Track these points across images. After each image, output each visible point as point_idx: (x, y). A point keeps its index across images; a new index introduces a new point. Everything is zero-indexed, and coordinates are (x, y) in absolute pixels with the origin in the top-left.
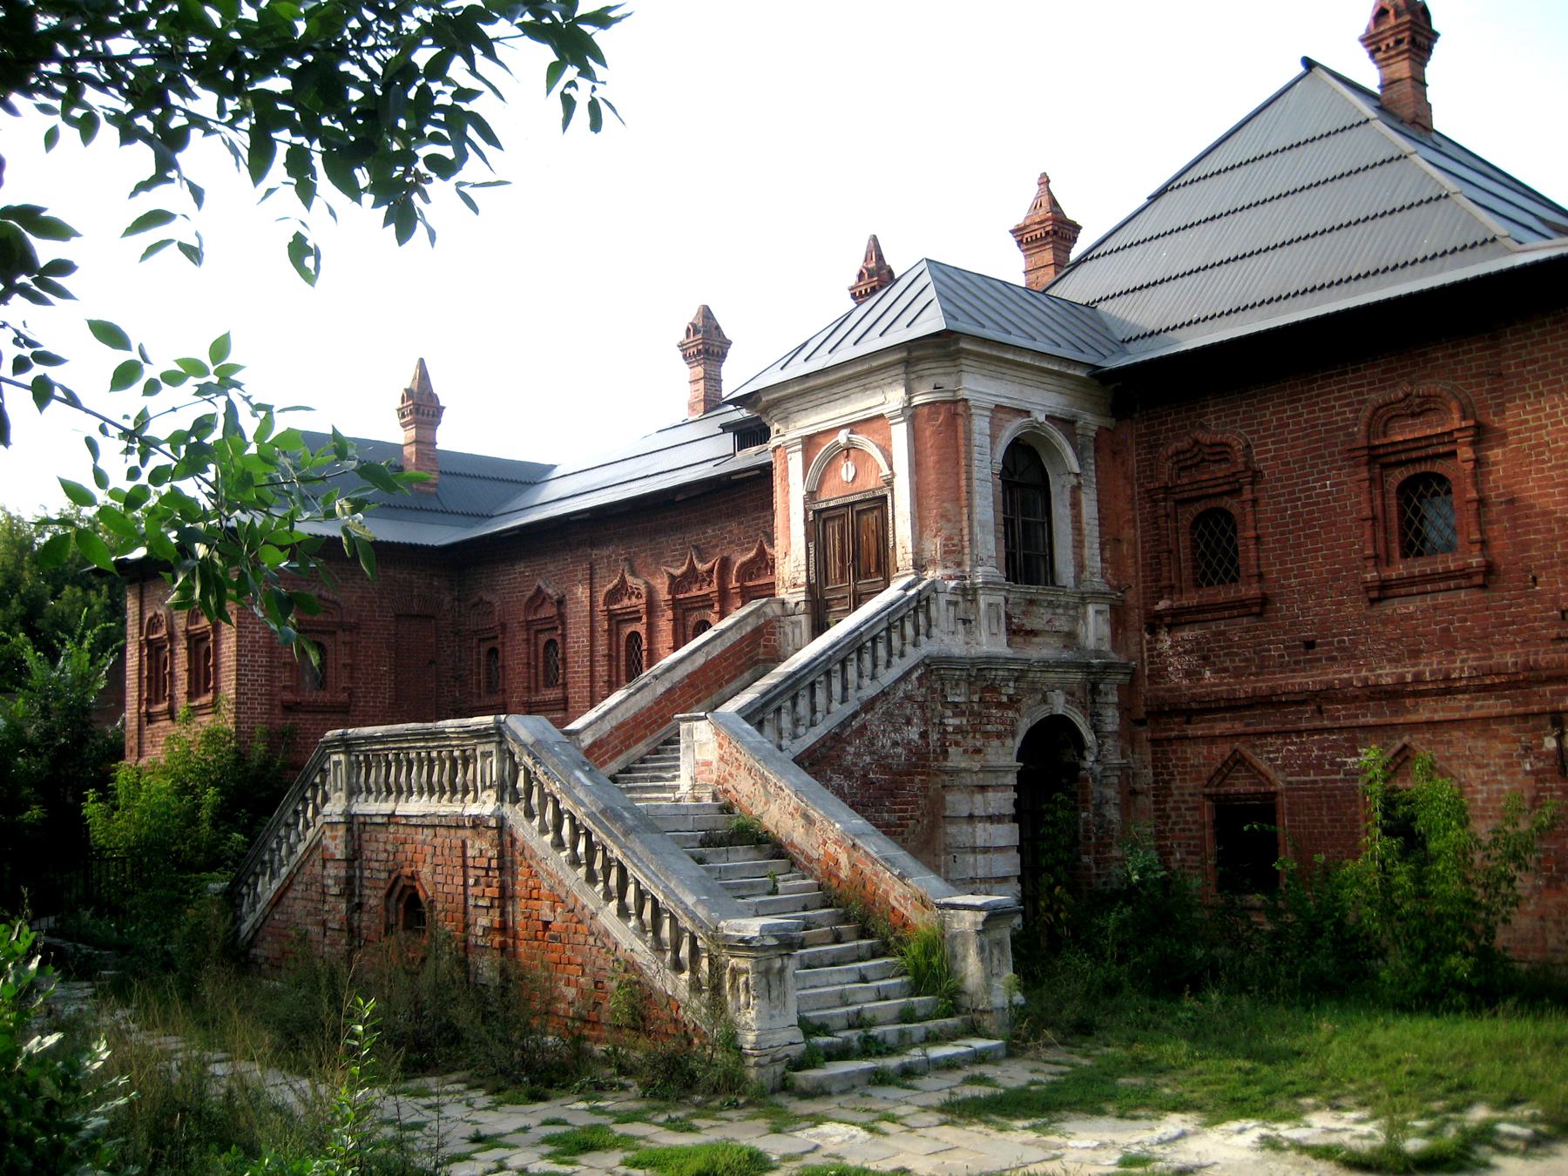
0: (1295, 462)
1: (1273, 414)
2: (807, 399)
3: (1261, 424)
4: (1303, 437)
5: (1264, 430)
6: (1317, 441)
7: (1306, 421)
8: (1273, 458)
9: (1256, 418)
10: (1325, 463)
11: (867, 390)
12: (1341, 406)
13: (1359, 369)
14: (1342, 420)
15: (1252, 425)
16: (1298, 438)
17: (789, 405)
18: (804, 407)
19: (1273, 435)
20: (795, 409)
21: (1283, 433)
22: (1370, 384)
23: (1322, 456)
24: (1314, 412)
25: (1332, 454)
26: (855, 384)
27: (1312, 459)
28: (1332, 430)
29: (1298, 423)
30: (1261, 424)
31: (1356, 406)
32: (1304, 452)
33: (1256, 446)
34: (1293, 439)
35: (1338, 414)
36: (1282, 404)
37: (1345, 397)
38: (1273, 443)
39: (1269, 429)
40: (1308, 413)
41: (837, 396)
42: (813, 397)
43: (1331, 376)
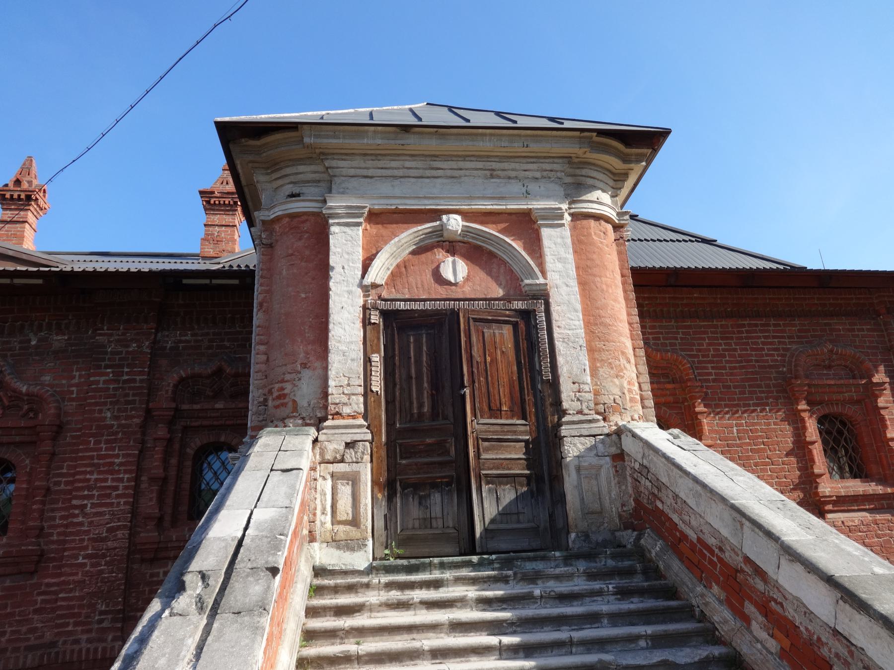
0: (735, 387)
1: (709, 344)
2: (381, 164)
3: (700, 350)
4: (741, 367)
5: (703, 356)
6: (752, 373)
7: (740, 356)
8: (714, 380)
9: (694, 345)
10: (763, 392)
11: (492, 176)
12: (769, 350)
13: (779, 325)
14: (772, 361)
15: (692, 350)
16: (735, 368)
17: (341, 164)
18: (370, 173)
19: (710, 362)
20: (352, 172)
21: (721, 362)
22: (789, 337)
23: (759, 386)
24: (746, 350)
25: (768, 386)
26: (480, 165)
27: (750, 386)
28: (764, 367)
29: (734, 356)
30: (700, 350)
31: (782, 352)
32: (743, 380)
33: (697, 368)
34: (731, 368)
35: (767, 355)
36: (717, 338)
37: (771, 344)
38: (713, 368)
39: (708, 356)
40: (741, 350)
41: (440, 173)
42: (394, 164)
43: (756, 325)
